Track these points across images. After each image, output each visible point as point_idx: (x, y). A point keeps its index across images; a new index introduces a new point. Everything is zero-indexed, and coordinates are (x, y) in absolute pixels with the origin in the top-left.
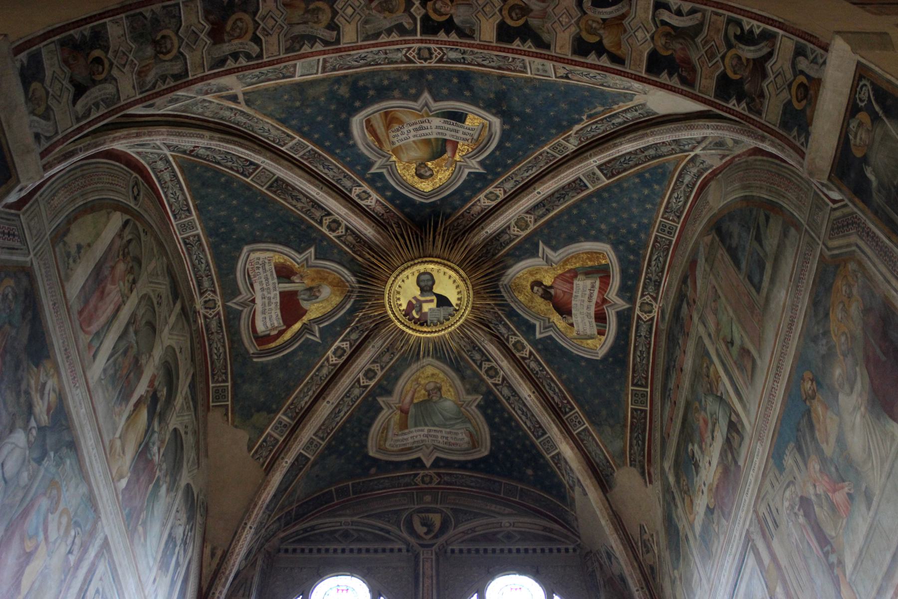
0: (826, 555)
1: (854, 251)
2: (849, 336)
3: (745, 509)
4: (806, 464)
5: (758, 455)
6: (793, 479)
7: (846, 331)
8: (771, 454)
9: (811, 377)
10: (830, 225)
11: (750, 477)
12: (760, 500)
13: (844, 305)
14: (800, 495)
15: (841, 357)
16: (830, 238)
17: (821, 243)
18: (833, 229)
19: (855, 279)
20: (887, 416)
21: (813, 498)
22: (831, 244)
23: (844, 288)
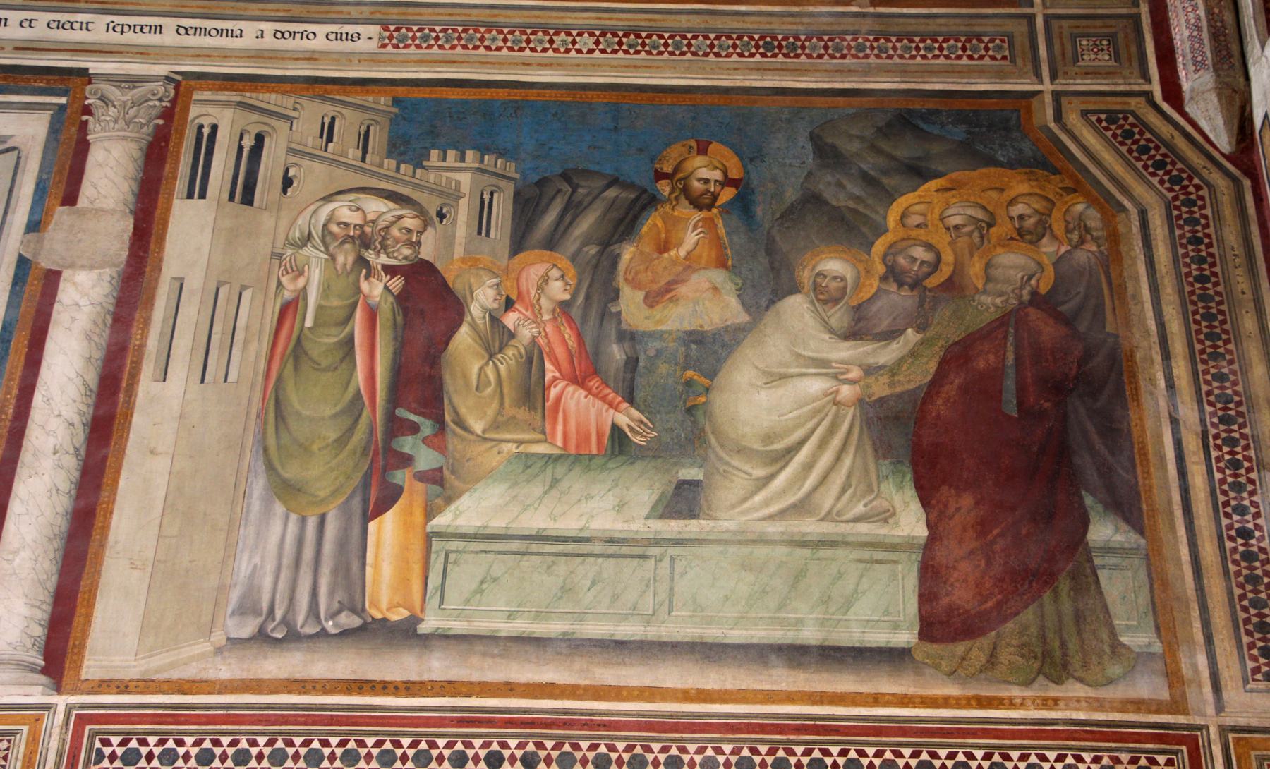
0: (396, 427)
1: (1123, 209)
2: (945, 271)
3: (130, 37)
4: (518, 245)
5: (339, 37)
6: (433, 213)
7: (948, 257)
8: (401, 91)
9: (735, 174)
10: (1114, 104)
11: (250, 28)
12: (235, 97)
13: (990, 225)
14: (426, 253)
15: (880, 269)
16: (1085, 114)
17: (1047, 86)
18: (1112, 117)
19: (1075, 237)
20: (909, 476)
21: (475, 310)
22: (1073, 119)
23: (1019, 209)
